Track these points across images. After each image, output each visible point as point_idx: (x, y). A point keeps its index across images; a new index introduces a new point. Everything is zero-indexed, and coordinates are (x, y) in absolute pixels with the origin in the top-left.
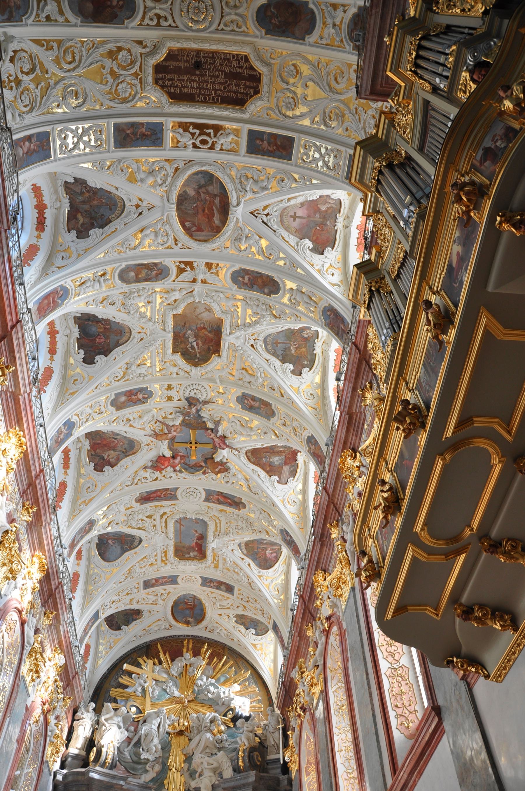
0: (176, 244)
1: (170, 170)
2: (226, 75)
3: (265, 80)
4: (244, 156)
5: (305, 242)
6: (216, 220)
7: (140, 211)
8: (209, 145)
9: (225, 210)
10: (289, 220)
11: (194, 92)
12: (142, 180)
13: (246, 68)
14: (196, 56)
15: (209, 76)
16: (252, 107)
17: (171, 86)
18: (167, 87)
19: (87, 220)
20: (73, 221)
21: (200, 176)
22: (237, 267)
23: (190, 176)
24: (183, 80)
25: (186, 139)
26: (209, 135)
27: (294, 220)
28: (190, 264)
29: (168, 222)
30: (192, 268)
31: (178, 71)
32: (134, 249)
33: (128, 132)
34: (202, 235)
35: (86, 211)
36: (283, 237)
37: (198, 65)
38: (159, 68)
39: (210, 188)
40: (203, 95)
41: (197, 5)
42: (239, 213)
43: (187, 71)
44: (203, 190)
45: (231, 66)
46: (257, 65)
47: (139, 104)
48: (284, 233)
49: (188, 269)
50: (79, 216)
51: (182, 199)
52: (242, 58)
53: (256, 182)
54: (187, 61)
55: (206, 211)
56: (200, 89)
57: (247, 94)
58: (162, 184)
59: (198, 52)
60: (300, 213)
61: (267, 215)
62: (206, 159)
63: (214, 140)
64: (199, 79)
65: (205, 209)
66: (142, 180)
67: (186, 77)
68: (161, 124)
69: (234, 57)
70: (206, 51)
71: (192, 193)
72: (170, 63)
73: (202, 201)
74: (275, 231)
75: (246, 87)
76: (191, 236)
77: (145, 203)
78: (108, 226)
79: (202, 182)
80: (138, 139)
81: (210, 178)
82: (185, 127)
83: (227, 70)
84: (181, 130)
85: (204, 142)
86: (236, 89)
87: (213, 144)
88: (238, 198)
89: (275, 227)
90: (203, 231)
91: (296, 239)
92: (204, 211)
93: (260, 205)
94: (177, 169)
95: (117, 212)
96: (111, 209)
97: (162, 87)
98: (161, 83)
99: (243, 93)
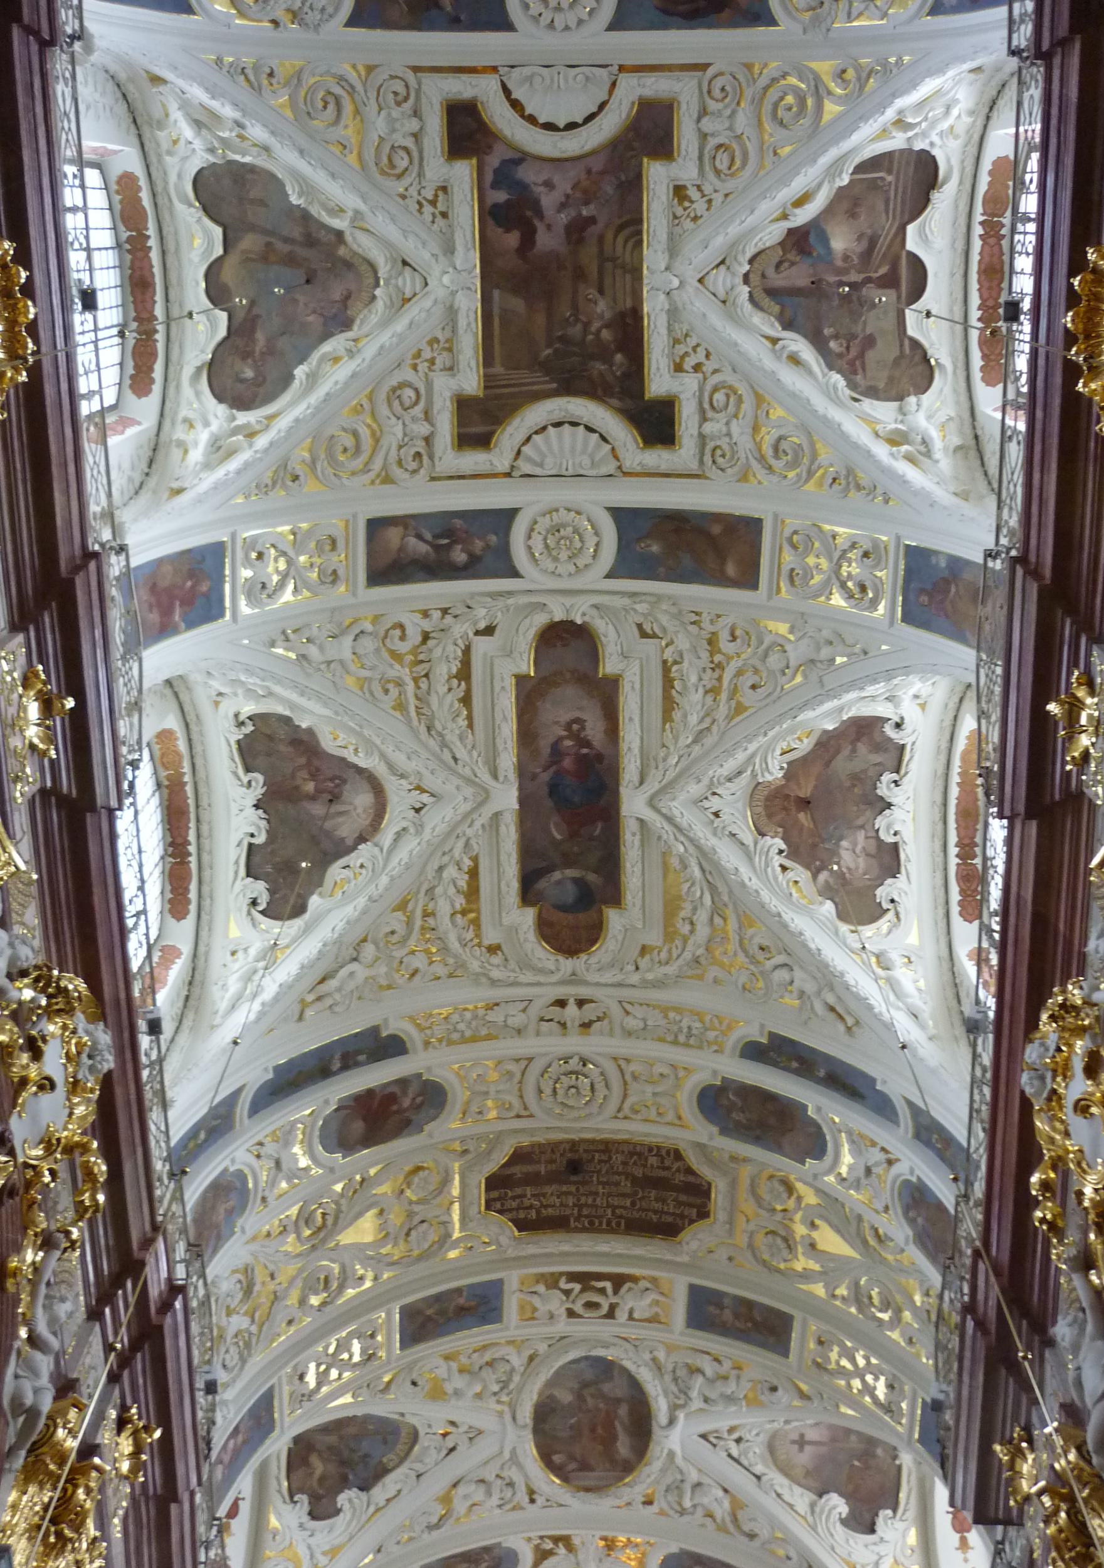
0: (532, 1501)
1: (517, 1361)
2: (635, 1181)
3: (719, 1198)
4: (682, 1334)
5: (832, 1503)
6: (623, 1447)
7: (451, 1445)
8: (605, 1309)
9: (642, 1427)
10: (787, 1451)
11: (568, 1212)
12: (457, 1393)
13: (678, 1170)
14: (571, 1150)
15: (599, 1183)
16: (694, 1245)
17: (518, 1209)
18: (510, 1210)
19: (332, 1469)
20: (300, 1473)
21: (583, 1365)
22: (674, 1549)
23: (562, 1367)
24: (544, 1195)
25: (555, 1303)
26: (602, 1291)
27: (801, 1449)
28: (565, 1540)
29: (514, 1459)
30: (570, 1548)
31: (532, 1179)
32: (437, 1526)
33: (429, 1312)
34: (590, 1478)
35: (330, 1448)
36: (779, 1495)
37: (574, 1167)
38: (493, 1183)
39: (606, 1387)
40: (586, 1216)
41: (573, 1082)
42: (675, 1439)
43: (553, 1178)
44: (592, 1390)
45: (645, 1166)
46: (705, 1172)
47: (453, 1254)
48: (780, 1482)
49: (562, 1550)
50: (314, 1459)
51: (544, 1413)
52: (668, 1153)
53: (711, 1381)
54: (552, 1161)
55: (600, 1430)
56: (580, 1207)
57: (682, 1216)
58: (502, 1389)
59: (574, 1145)
60: (812, 1435)
61: (738, 1441)
62: (596, 1337)
63: (614, 1300)
64: (578, 1189)
65: (595, 1430)
66: (457, 1393)
67: (548, 1189)
68: (500, 1282)
69: (650, 1149)
70: (592, 1142)
71: (565, 1397)
72: (518, 1170)
73: (589, 1411)
74: (758, 1478)
75: (680, 1204)
76: (565, 1479)
77: (465, 1428)
78: (380, 1484)
79: (589, 1375)
80: (449, 1319)
81: (606, 1368)
82: (551, 1281)
83: (638, 1172)
84: (541, 1288)
85: (591, 1305)
86: (657, 1206)
87: (613, 1308)
88: (674, 1408)
89: (759, 1469)
90: (592, 1470)
91: (810, 1496)
92: (593, 1430)
93: (723, 1425)
94: (531, 1359)
95: (400, 1448)
96: (385, 1442)
97: (500, 1212)
98: (498, 1205)
99: (673, 1214)
